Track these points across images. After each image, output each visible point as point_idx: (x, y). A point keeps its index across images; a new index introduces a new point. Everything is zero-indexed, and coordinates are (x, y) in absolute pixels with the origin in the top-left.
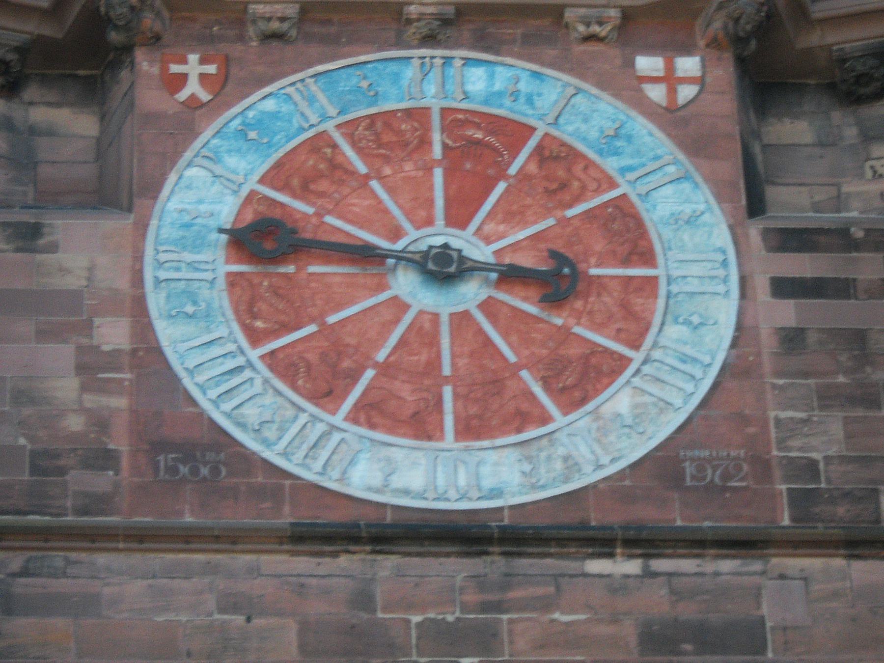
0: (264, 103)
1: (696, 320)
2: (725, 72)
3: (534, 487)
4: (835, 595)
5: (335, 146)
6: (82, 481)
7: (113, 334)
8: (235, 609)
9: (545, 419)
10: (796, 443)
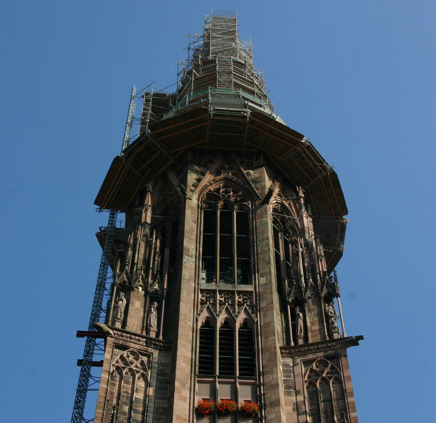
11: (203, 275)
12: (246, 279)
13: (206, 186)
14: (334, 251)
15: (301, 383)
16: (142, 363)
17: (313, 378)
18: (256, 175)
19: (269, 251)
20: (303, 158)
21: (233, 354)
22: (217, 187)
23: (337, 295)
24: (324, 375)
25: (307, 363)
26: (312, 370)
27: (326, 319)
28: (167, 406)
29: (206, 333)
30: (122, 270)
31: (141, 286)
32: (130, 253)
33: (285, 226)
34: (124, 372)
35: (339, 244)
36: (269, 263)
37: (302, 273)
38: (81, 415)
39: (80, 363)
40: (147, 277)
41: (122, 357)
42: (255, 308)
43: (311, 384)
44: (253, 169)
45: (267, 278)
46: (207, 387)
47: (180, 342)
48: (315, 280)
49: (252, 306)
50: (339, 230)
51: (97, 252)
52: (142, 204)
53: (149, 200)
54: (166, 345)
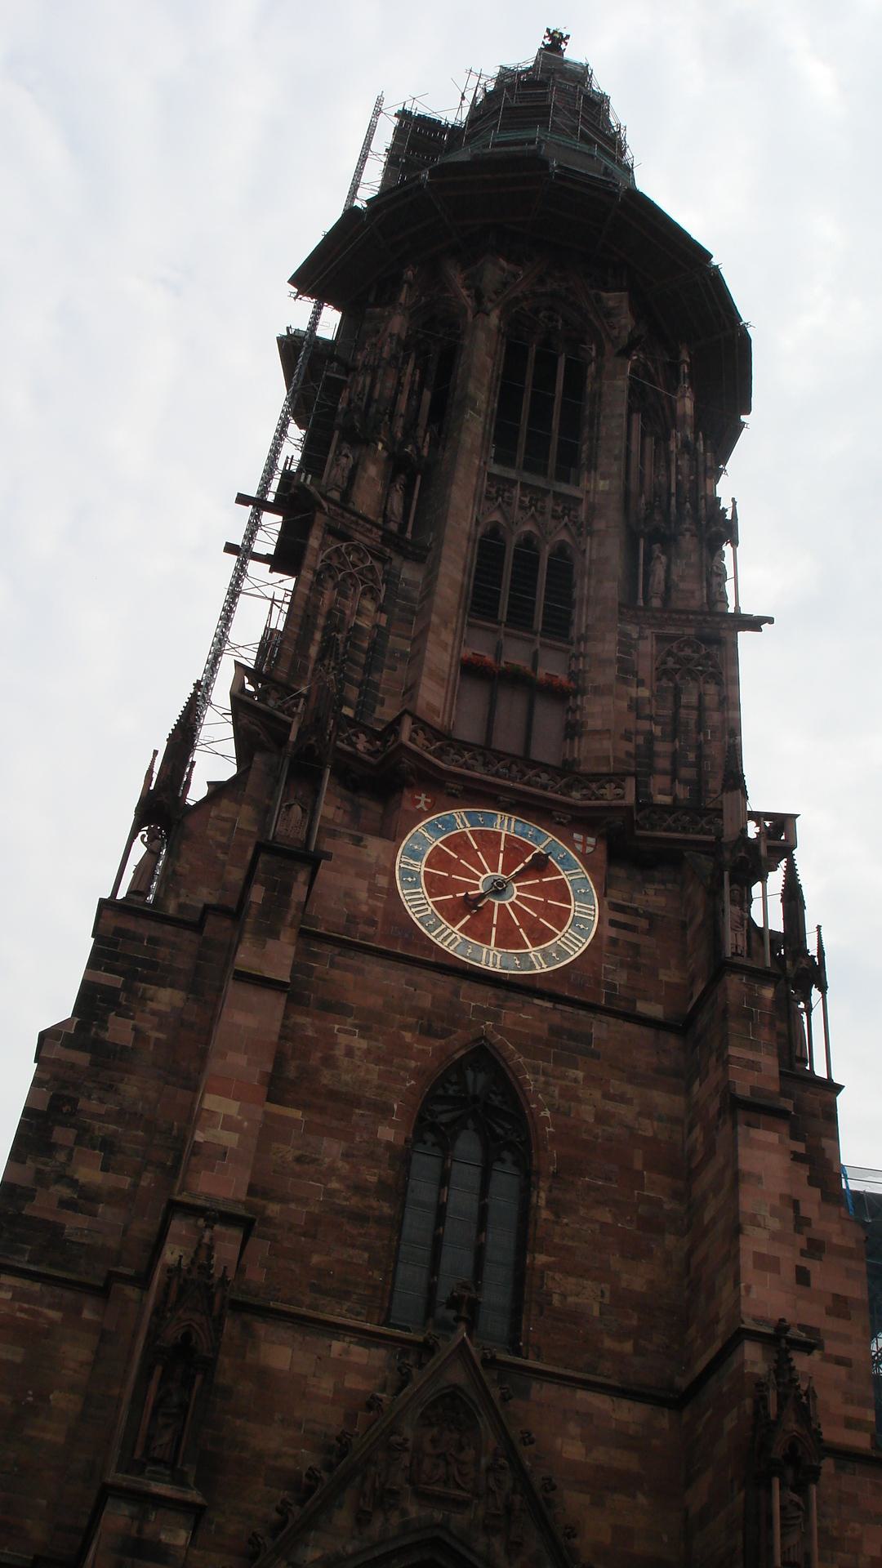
2: (602, 847)
6: (362, 928)
7: (382, 881)
12: (562, 476)
47: (447, 551)
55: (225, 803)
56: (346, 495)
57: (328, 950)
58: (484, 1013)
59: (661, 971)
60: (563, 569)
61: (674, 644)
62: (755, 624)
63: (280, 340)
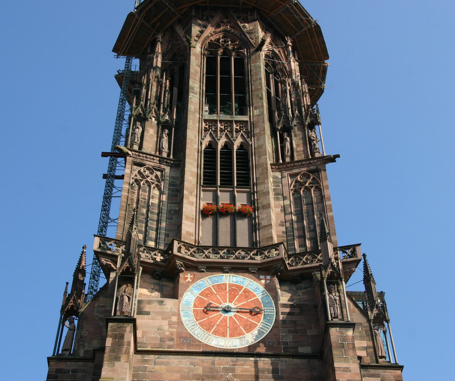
0: (199, 282)
1: (269, 318)
3: (242, 345)
4: (290, 364)
5: (211, 289)
6: (168, 343)
7: (174, 319)
8: (192, 365)
9: (244, 334)
10: (284, 339)
11: (206, 108)
12: (242, 111)
13: (208, 37)
14: (317, 89)
15: (288, 191)
16: (156, 176)
17: (298, 187)
18: (251, 28)
19: (261, 89)
20: (291, 13)
21: (232, 169)
22: (218, 37)
23: (319, 124)
24: (307, 185)
25: (292, 176)
26: (297, 181)
27: (309, 143)
28: (177, 209)
29: (209, 153)
30: (137, 104)
31: (154, 117)
32: (144, 91)
33: (275, 69)
34: (142, 183)
35: (321, 83)
36: (261, 98)
37: (290, 106)
38: (107, 215)
39: (105, 176)
40: (159, 110)
41: (139, 172)
42: (250, 134)
43: (296, 192)
44: (248, 22)
45: (260, 111)
46: (210, 195)
48: (300, 111)
49: (247, 133)
50: (321, 72)
51: (116, 91)
52: (153, 51)
53: (159, 48)
54: (176, 163)
55: (101, 299)
56: (141, 147)
57: (152, 357)
58: (227, 370)
59: (308, 331)
60: (245, 153)
61: (299, 177)
62: (332, 159)
63: (116, 77)
